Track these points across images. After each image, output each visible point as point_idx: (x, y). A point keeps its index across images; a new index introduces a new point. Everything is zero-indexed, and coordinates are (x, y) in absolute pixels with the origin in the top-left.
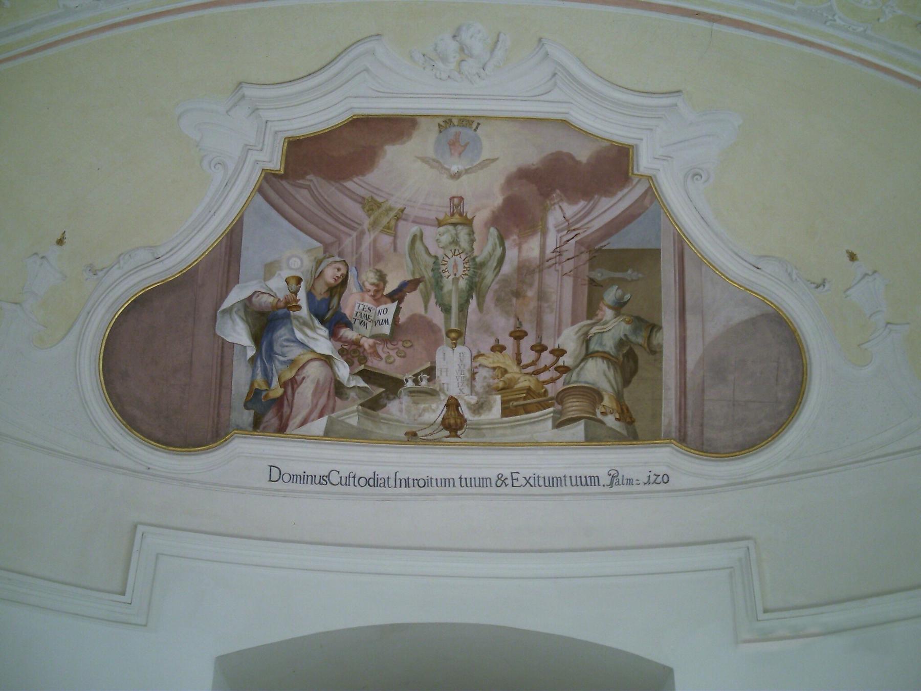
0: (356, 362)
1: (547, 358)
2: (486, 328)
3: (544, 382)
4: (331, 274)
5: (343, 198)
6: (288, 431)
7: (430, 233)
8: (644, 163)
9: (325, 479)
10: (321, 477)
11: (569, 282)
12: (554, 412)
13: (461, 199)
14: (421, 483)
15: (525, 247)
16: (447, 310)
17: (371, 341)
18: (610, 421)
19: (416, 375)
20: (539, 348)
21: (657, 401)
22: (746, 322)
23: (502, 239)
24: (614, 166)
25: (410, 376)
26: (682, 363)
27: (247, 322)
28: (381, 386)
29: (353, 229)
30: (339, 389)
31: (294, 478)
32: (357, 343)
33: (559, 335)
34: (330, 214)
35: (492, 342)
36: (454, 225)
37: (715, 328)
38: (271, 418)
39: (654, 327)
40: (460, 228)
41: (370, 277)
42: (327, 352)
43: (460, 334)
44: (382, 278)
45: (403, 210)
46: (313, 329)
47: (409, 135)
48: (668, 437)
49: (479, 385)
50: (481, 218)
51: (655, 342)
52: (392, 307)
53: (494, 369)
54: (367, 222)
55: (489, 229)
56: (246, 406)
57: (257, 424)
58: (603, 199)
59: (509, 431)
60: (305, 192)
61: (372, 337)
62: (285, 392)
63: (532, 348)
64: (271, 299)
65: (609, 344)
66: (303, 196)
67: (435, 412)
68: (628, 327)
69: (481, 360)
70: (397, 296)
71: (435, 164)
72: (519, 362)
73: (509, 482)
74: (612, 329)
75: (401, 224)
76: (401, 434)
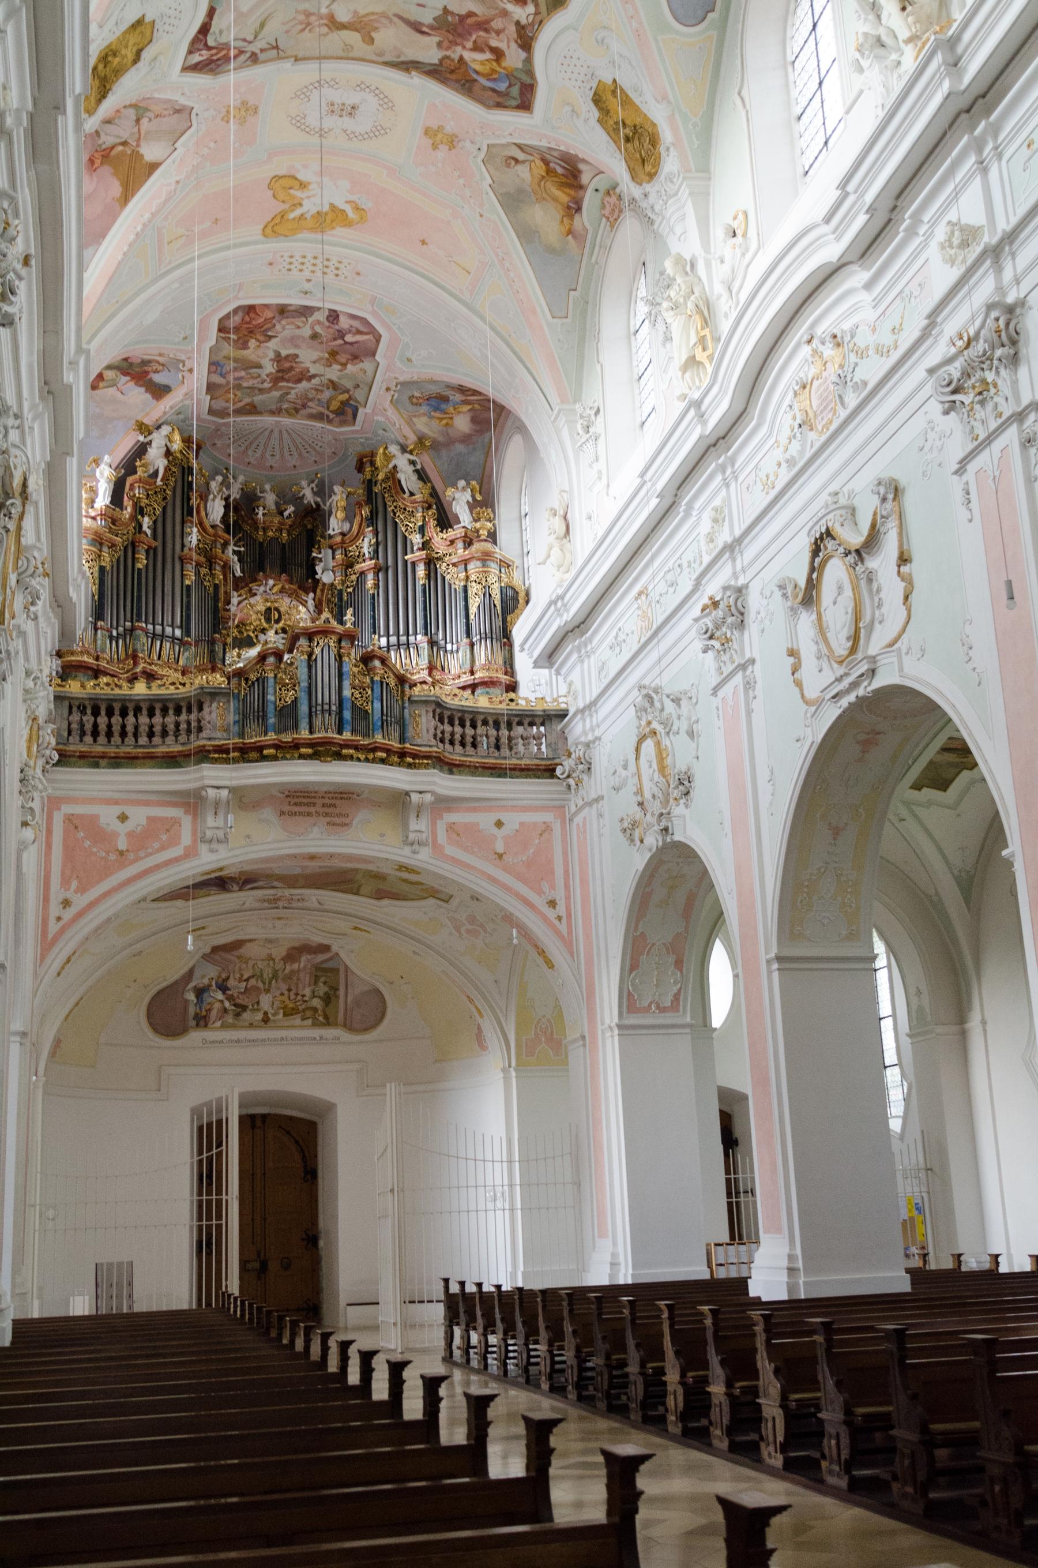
1: (299, 998)
2: (278, 988)
4: (224, 976)
7: (260, 964)
9: (221, 1042)
16: (264, 983)
18: (321, 1018)
20: (297, 994)
30: (226, 1010)
38: (202, 1023)
39: (337, 989)
41: (238, 976)
44: (242, 975)
57: (197, 1025)
65: (321, 994)
66: (217, 957)
67: (259, 1016)
74: (322, 989)
76: (247, 1024)
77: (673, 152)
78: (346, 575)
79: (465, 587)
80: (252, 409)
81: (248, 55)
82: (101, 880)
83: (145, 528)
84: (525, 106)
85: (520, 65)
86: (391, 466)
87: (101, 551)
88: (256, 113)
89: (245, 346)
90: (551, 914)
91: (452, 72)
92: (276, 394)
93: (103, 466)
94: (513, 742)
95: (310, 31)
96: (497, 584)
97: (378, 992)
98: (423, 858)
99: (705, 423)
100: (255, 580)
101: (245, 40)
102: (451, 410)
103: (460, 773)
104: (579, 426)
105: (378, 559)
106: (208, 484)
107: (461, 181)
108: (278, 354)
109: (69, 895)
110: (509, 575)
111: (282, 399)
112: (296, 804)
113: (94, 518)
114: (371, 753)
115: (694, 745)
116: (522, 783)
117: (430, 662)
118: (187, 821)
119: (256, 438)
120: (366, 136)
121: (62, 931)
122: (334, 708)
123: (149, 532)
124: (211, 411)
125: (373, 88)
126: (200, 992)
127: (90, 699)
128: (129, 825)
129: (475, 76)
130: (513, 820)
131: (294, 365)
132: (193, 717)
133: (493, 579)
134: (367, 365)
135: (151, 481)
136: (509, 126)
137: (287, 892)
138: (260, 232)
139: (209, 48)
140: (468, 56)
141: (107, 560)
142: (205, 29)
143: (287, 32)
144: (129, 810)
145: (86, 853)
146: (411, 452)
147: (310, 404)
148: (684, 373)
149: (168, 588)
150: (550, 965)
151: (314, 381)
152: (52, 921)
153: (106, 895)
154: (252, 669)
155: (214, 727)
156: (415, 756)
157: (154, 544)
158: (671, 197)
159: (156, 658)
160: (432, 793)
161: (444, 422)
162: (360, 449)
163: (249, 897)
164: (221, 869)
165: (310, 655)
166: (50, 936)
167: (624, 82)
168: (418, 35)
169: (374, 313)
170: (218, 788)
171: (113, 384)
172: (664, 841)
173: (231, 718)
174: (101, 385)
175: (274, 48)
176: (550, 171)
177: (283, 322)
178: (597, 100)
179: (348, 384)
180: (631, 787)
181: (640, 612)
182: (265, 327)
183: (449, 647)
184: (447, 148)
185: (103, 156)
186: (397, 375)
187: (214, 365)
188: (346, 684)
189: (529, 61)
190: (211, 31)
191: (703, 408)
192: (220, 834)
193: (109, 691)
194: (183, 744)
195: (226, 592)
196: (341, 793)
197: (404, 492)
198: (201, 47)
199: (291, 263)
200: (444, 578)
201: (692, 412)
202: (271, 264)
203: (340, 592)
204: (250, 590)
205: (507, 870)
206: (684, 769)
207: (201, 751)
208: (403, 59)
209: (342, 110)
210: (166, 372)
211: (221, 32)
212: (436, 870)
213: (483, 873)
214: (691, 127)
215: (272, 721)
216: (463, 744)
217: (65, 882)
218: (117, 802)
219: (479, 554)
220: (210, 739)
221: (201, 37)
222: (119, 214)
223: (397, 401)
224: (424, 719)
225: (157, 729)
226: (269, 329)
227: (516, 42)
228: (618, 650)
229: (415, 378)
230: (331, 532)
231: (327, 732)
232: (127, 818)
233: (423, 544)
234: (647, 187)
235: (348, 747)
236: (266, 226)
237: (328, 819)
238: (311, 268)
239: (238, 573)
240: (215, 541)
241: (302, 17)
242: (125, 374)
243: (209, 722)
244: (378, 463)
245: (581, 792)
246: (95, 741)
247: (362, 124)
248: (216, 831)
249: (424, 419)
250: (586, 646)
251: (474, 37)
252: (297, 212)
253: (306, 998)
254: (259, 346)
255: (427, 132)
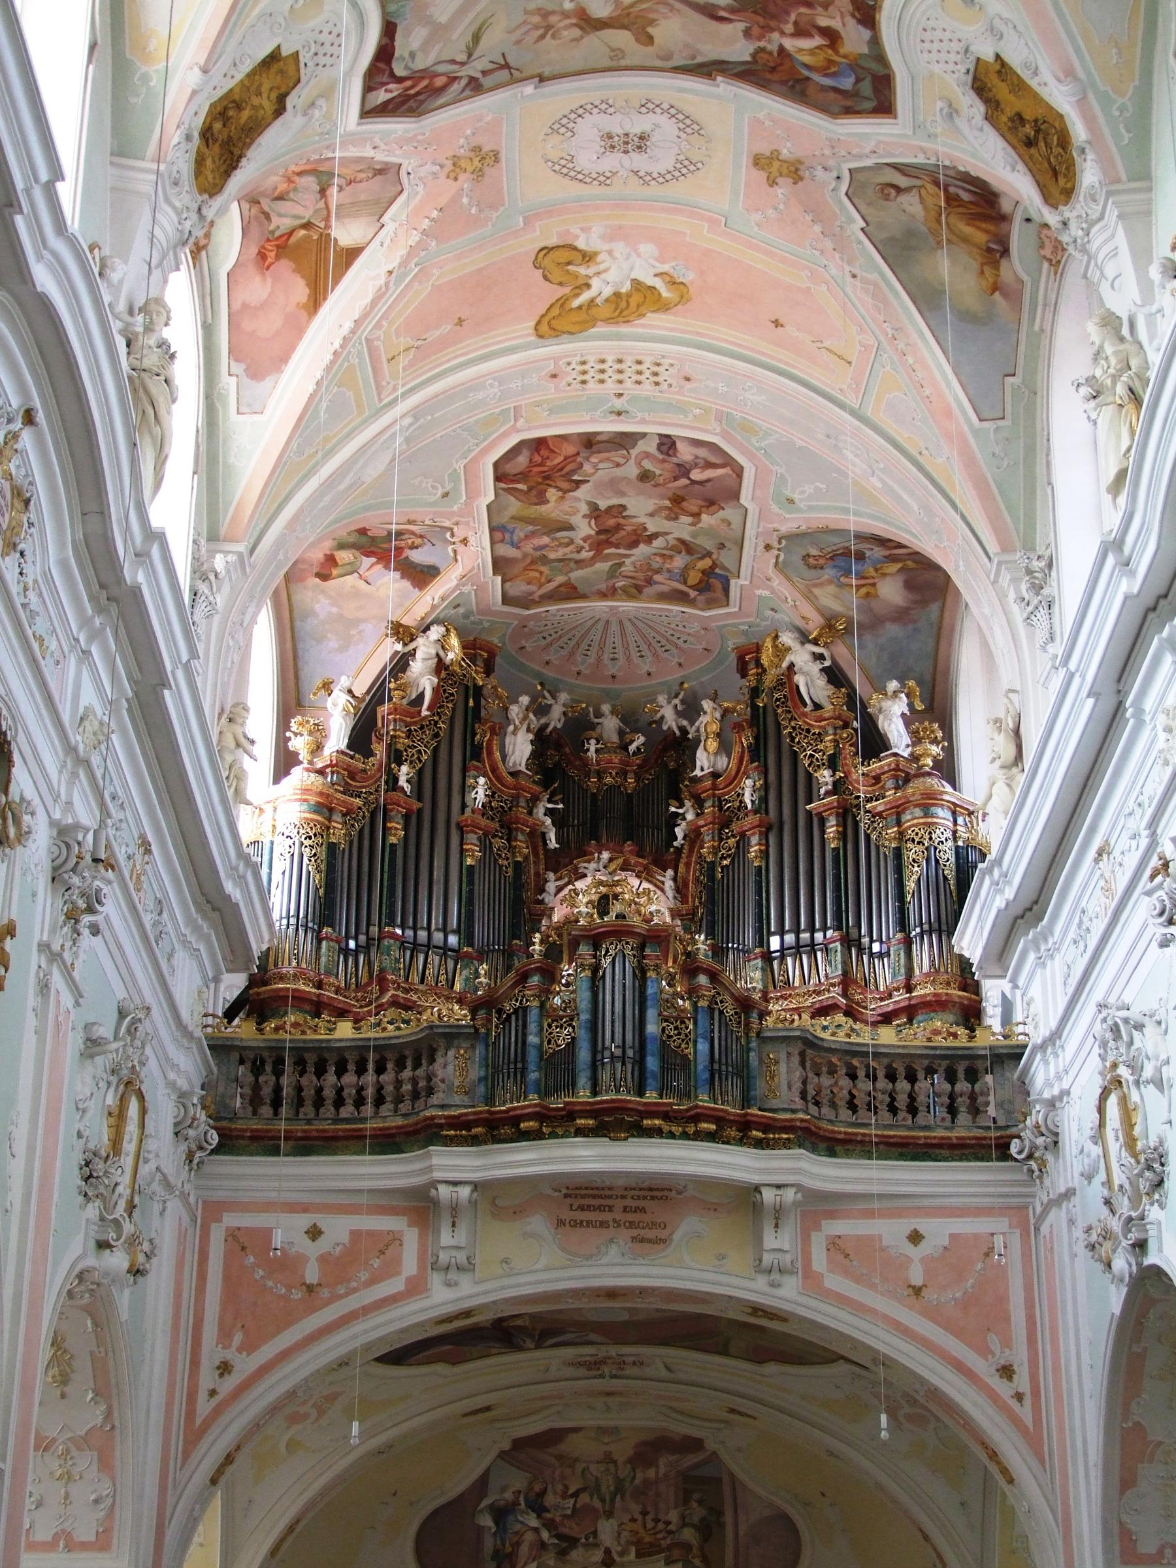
1: (661, 1526)
4: (537, 1488)
7: (593, 1468)
16: (603, 1500)
20: (656, 1520)
26: (736, 1533)
30: (543, 1545)
32: (553, 1520)
39: (721, 1513)
41: (560, 1487)
44: (566, 1487)
49: (623, 1541)
50: (621, 1460)
52: (572, 1501)
65: (696, 1519)
74: (697, 1513)
77: (1090, 156)
78: (721, 839)
79: (898, 853)
80: (570, 592)
81: (464, 82)
82: (279, 1330)
83: (402, 782)
84: (884, 107)
85: (865, 50)
86: (785, 665)
87: (330, 820)
88: (497, 160)
89: (542, 500)
90: (1004, 1389)
91: (773, 70)
92: (603, 566)
93: (336, 692)
94: (980, 1099)
95: (553, 37)
96: (950, 843)
97: (786, 1518)
98: (788, 1295)
99: (1132, 574)
100: (583, 854)
101: (453, 62)
102: (873, 573)
103: (848, 1154)
104: (1024, 587)
105: (767, 813)
106: (506, 709)
107: (818, 228)
108: (594, 507)
109: (230, 1355)
110: (970, 827)
111: (613, 573)
112: (582, 1208)
113: (321, 772)
114: (688, 1125)
115: (1165, 1102)
116: (953, 1169)
117: (846, 974)
118: (411, 1237)
119: (583, 637)
120: (668, 177)
121: (217, 1412)
122: (630, 1053)
123: (407, 787)
124: (506, 600)
125: (665, 106)
126: (501, 1514)
127: (271, 1048)
128: (323, 1245)
129: (806, 73)
130: (938, 1232)
131: (621, 521)
132: (420, 1072)
133: (942, 833)
134: (729, 513)
135: (412, 710)
136: (868, 138)
137: (613, 1351)
138: (532, 331)
139: (400, 80)
140: (789, 44)
141: (338, 832)
142: (385, 54)
143: (518, 42)
144: (325, 1221)
145: (255, 1288)
146: (815, 642)
147: (657, 578)
148: (1115, 497)
149: (438, 874)
150: (1011, 1481)
151: (658, 543)
152: (202, 1396)
153: (285, 1355)
154: (507, 996)
155: (450, 1088)
156: (766, 1127)
157: (416, 805)
158: (1093, 224)
159: (417, 980)
160: (799, 1187)
161: (863, 591)
162: (741, 641)
163: (554, 1358)
164: (467, 1314)
165: (595, 968)
166: (198, 1421)
167: (1014, 60)
168: (714, 23)
169: (725, 435)
170: (455, 1183)
171: (353, 570)
172: (1139, 1264)
173: (476, 1072)
174: (335, 572)
175: (502, 67)
176: (951, 200)
177: (594, 459)
178: (980, 88)
179: (708, 544)
180: (1102, 1176)
181: (1102, 883)
182: (567, 469)
183: (876, 947)
184: (791, 180)
185: (278, 247)
186: (776, 525)
187: (497, 531)
188: (651, 1014)
189: (875, 41)
190: (397, 54)
191: (1127, 549)
192: (461, 1257)
193: (299, 1037)
194: (405, 1115)
195: (537, 874)
196: (651, 1189)
197: (805, 705)
198: (385, 79)
199: (584, 373)
200: (868, 837)
201: (1111, 560)
202: (554, 376)
203: (712, 865)
204: (576, 868)
205: (933, 1314)
206: (1153, 1141)
207: (430, 1126)
208: (699, 60)
209: (627, 143)
210: (427, 547)
211: (412, 55)
212: (809, 1315)
213: (886, 1318)
214: (1117, 113)
215: (533, 1076)
216: (852, 1107)
217: (225, 1336)
218: (305, 1209)
219: (917, 797)
220: (443, 1107)
221: (382, 65)
222: (307, 327)
223: (784, 562)
224: (783, 1067)
225: (370, 1092)
226: (574, 472)
227: (853, 16)
228: (1082, 944)
229: (803, 528)
230: (698, 773)
231: (618, 1091)
232: (320, 1233)
233: (835, 784)
234: (1067, 212)
235: (652, 1115)
236: (538, 323)
237: (634, 1232)
238: (617, 377)
239: (553, 844)
240: (516, 797)
241: (536, 19)
242: (368, 554)
243: (443, 1081)
244: (765, 661)
245: (1047, 1182)
246: (276, 1113)
247: (661, 159)
248: (454, 1253)
249: (831, 589)
250: (1046, 940)
251: (793, 17)
252: (585, 297)
253: (672, 1527)
254: (562, 498)
255: (758, 161)
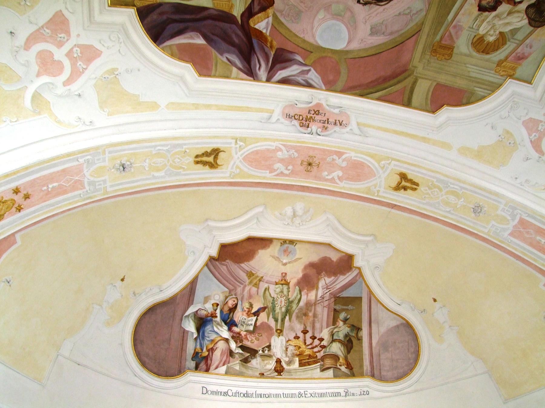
0: (238, 341)
1: (316, 342)
2: (292, 329)
3: (316, 352)
4: (231, 303)
5: (239, 270)
6: (210, 371)
7: (272, 287)
8: (358, 262)
9: (226, 394)
10: (224, 393)
11: (326, 310)
12: (320, 365)
13: (286, 274)
14: (267, 396)
15: (309, 295)
16: (276, 320)
17: (245, 333)
18: (343, 368)
19: (263, 348)
20: (313, 338)
21: (361, 360)
22: (395, 326)
23: (300, 291)
24: (346, 263)
25: (260, 349)
27: (195, 322)
28: (248, 352)
29: (242, 284)
30: (231, 353)
31: (213, 393)
32: (239, 333)
33: (321, 331)
34: (233, 277)
35: (294, 335)
36: (282, 284)
37: (383, 330)
38: (203, 365)
39: (359, 329)
40: (284, 286)
41: (246, 305)
42: (227, 337)
43: (281, 331)
44: (251, 306)
45: (262, 277)
46: (222, 326)
47: (269, 247)
48: (367, 375)
50: (293, 282)
51: (359, 335)
52: (254, 318)
53: (295, 346)
54: (247, 283)
55: (295, 287)
56: (192, 359)
57: (197, 368)
58: (341, 276)
59: (302, 373)
60: (225, 267)
61: (245, 331)
62: (209, 354)
63: (311, 338)
64: (205, 312)
65: (341, 336)
66: (223, 269)
67: (271, 365)
68: (349, 329)
69: (290, 342)
70: (257, 314)
71: (277, 259)
72: (305, 343)
73: (303, 395)
74: (343, 330)
75: (261, 283)
97: (408, 326)
253: (324, 343)
